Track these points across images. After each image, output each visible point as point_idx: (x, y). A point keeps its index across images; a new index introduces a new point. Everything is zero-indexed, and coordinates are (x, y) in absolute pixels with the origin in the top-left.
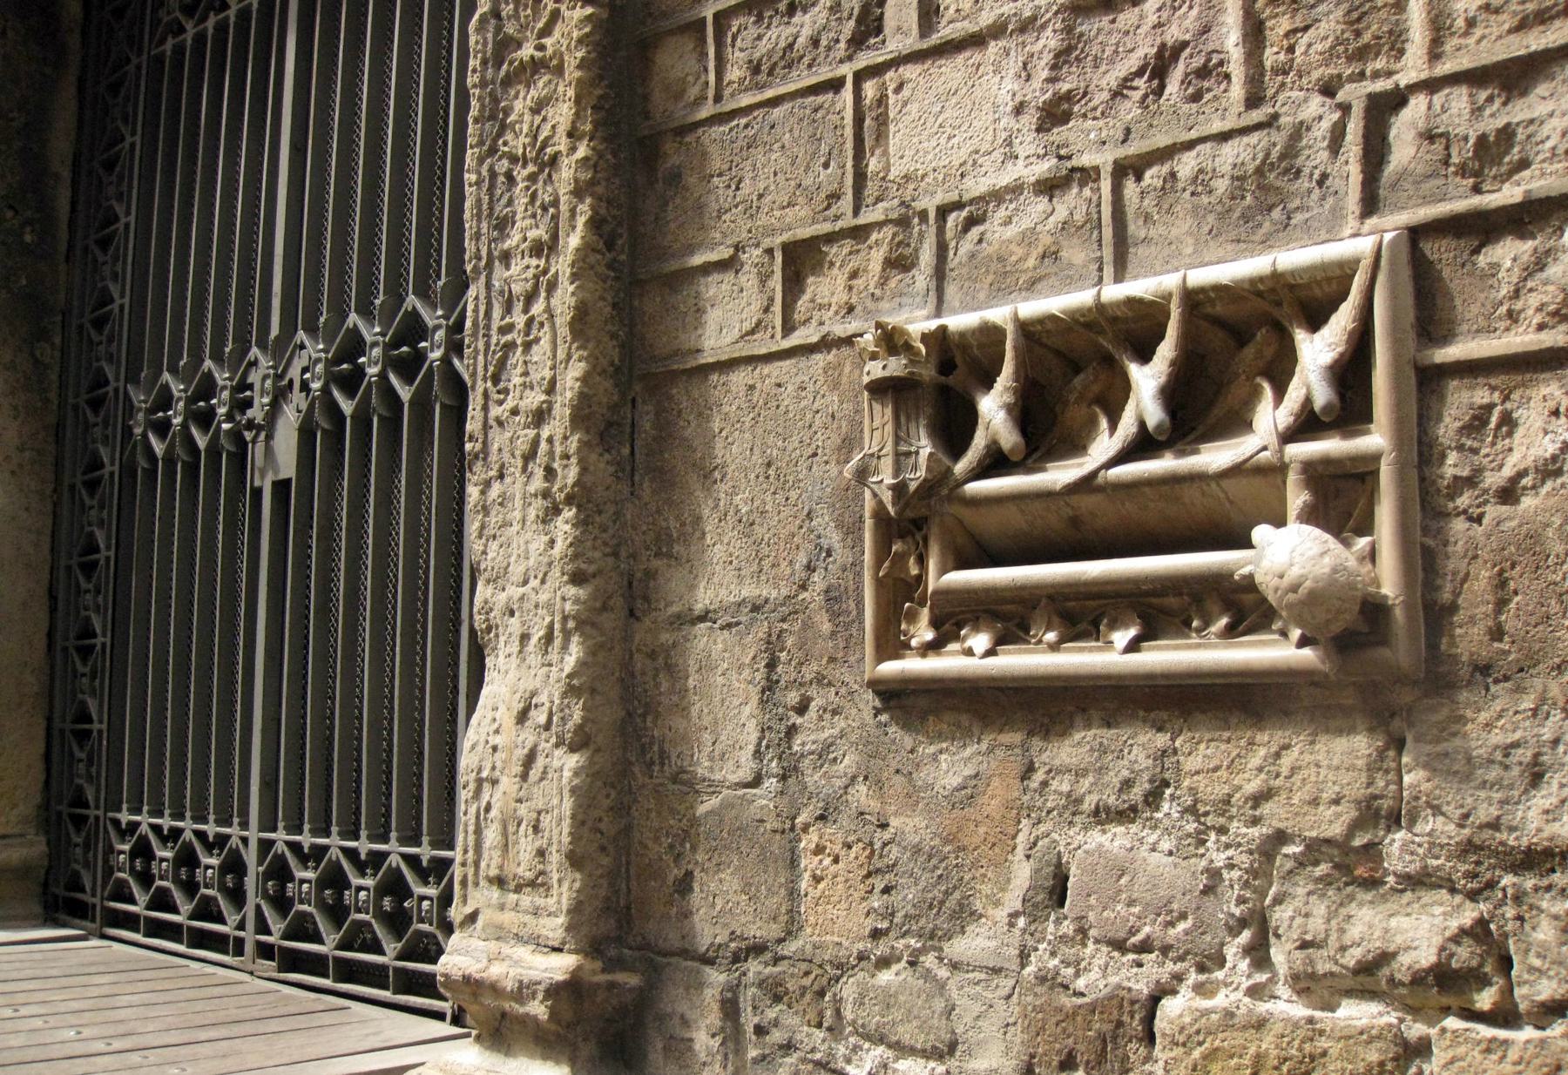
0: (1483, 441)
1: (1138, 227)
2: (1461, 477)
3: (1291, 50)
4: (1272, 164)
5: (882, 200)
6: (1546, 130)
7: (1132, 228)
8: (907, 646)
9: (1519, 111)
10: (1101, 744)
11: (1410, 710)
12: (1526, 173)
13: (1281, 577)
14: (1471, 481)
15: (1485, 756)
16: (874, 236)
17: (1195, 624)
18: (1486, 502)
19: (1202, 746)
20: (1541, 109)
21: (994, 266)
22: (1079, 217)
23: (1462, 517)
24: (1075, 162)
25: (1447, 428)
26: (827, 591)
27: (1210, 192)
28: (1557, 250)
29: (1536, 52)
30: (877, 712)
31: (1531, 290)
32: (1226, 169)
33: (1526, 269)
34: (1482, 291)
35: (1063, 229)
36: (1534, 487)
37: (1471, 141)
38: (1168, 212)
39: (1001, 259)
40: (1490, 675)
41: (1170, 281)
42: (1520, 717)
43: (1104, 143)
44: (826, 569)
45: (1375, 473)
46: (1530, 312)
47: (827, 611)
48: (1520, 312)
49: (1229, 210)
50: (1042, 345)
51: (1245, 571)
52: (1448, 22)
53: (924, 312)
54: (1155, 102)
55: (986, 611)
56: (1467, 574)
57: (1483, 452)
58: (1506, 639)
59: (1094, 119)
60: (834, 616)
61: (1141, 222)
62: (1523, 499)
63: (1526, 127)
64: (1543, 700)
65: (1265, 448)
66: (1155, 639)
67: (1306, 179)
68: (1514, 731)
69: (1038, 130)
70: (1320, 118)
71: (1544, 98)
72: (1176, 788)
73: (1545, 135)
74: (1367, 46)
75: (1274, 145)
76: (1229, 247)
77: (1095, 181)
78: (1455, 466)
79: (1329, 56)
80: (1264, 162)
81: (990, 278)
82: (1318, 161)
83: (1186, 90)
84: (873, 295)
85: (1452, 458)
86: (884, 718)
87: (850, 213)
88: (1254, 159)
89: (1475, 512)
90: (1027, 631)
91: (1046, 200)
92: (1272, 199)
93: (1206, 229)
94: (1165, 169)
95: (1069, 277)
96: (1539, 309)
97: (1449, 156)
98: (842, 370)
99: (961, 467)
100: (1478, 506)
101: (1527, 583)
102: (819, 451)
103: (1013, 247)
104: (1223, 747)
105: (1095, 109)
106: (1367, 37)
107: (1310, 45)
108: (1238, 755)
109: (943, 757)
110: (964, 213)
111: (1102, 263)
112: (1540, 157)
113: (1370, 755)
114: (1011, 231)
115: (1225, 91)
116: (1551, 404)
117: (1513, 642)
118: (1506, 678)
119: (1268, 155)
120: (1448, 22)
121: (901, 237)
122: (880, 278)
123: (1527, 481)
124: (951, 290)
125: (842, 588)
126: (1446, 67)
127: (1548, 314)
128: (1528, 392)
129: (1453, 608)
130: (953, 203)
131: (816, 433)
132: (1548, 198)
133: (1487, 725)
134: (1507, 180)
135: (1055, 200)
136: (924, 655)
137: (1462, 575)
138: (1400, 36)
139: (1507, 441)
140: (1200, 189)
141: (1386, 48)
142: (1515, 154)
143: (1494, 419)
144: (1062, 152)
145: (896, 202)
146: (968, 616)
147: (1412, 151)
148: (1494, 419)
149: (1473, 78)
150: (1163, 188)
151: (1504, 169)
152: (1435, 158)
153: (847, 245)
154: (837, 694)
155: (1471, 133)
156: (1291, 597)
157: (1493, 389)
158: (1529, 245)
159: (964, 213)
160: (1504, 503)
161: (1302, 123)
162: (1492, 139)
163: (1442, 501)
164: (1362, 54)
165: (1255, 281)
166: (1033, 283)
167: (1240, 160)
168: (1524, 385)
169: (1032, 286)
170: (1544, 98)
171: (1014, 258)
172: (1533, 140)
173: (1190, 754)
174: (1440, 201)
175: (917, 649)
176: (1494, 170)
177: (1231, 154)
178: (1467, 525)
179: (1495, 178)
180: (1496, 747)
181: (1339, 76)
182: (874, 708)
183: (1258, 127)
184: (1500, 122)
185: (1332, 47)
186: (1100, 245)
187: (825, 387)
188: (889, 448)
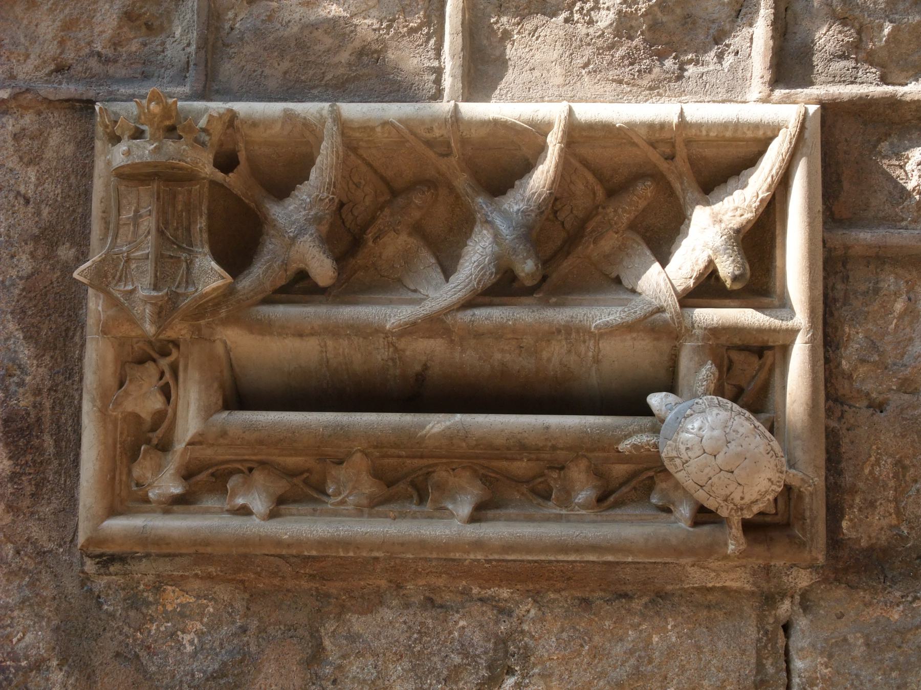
50: (360, 156)
51: (643, 439)
53: (187, 89)
55: (262, 463)
72: (523, 678)
76: (611, 87)
81: (285, 65)
84: (99, 55)
93: (580, 61)
98: (45, 142)
99: (246, 283)
103: (319, 34)
109: (187, 637)
125: (32, 419)
136: (166, 512)
146: (239, 466)
152: (846, 39)
165: (651, 127)
174: (852, 83)
175: (159, 502)
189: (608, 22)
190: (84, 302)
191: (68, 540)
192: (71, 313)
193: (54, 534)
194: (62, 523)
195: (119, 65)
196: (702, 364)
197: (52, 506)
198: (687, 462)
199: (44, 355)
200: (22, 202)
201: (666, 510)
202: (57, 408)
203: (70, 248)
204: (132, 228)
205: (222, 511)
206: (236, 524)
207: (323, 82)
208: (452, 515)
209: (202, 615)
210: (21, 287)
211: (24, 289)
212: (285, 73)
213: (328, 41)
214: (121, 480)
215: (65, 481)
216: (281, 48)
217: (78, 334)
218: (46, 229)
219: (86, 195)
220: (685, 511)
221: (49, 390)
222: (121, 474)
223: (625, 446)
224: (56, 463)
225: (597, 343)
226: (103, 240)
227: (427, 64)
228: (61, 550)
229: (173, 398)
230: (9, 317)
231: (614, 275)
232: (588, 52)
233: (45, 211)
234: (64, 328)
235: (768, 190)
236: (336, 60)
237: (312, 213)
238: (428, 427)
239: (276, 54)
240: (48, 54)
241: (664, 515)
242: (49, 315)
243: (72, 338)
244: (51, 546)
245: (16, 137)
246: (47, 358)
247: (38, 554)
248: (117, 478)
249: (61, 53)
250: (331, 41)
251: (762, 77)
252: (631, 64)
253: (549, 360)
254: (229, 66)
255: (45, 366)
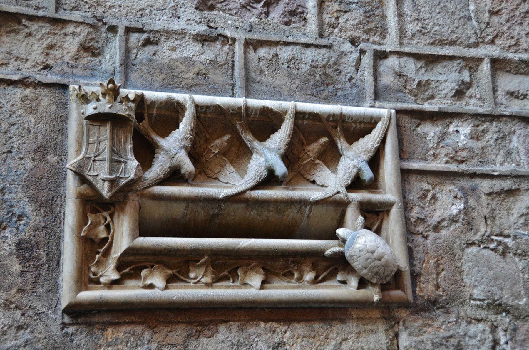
0: (425, 204)
1: (256, 75)
2: (421, 219)
3: (337, 18)
4: (330, 65)
5: (77, 10)
6: (442, 86)
7: (252, 74)
8: (98, 282)
9: (431, 76)
10: (238, 341)
11: (404, 322)
12: (434, 101)
13: (373, 253)
14: (423, 220)
15: (439, 342)
16: (71, 28)
17: (296, 275)
18: (429, 231)
19: (299, 341)
20: (441, 78)
21: (165, 70)
22: (221, 60)
23: (420, 236)
24: (220, 31)
25: (413, 196)
26: (18, 244)
27: (298, 69)
28: (448, 134)
29: (441, 55)
30: (64, 325)
31: (442, 147)
32: (309, 60)
33: (439, 138)
34: (421, 143)
35: (210, 63)
36: (447, 227)
37: (416, 82)
38: (273, 72)
39: (170, 68)
40: (435, 306)
41: (288, 105)
42: (450, 325)
43: (237, 28)
44: (18, 228)
45: (388, 212)
46: (443, 156)
47: (18, 257)
48: (438, 154)
49: (308, 80)
51: (337, 249)
52: (404, 32)
54: (266, 18)
56: (424, 261)
57: (426, 209)
58: (441, 290)
59: (230, 14)
60: (23, 261)
61: (258, 73)
62: (441, 231)
63: (435, 83)
64: (458, 318)
65: (338, 193)
66: (270, 283)
67: (344, 77)
68: (449, 331)
69: (196, 8)
70: (352, 53)
71: (441, 74)
73: (442, 88)
74: (371, 29)
75: (332, 57)
76: (308, 97)
77: (231, 45)
78: (418, 213)
79: (356, 27)
80: (327, 64)
81: (163, 76)
82: (349, 71)
83: (283, 18)
84: (68, 63)
85: (416, 210)
86: (70, 330)
87: (52, 9)
88: (322, 60)
89: (425, 234)
90: (188, 277)
91: (200, 45)
92: (328, 81)
93: (295, 86)
94: (273, 51)
95: (214, 89)
96: (447, 155)
97: (406, 85)
98: (39, 103)
100: (426, 232)
101: (447, 266)
102: (14, 150)
104: (311, 340)
105: (231, 9)
106: (371, 26)
107: (347, 20)
108: (320, 345)
110: (145, 36)
111: (233, 86)
112: (439, 96)
113: (388, 343)
114: (175, 55)
115: (303, 26)
116: (453, 194)
117: (444, 291)
118: (442, 307)
119: (329, 60)
120: (404, 32)
121: (93, 36)
122: (75, 55)
123: (445, 223)
124: (134, 76)
125: (33, 242)
126: (406, 49)
127: (450, 158)
128: (442, 187)
129: (419, 275)
130: (137, 29)
131: (11, 138)
132: (447, 112)
133: (438, 328)
134: (426, 101)
135: (205, 47)
137: (423, 260)
138: (384, 30)
139: (433, 206)
140: (292, 66)
141: (379, 33)
142: (429, 92)
143: (430, 196)
144: (212, 25)
145: (89, 14)
147: (392, 79)
148: (430, 196)
149: (417, 57)
150: (271, 60)
151: (425, 97)
153: (47, 28)
154: (23, 315)
155: (416, 79)
156: (377, 263)
157: (429, 184)
158: (437, 129)
159: (145, 36)
160: (435, 232)
161: (343, 52)
162: (423, 83)
163: (413, 228)
164: (368, 31)
166: (192, 86)
167: (316, 59)
168: (440, 184)
169: (190, 88)
170: (441, 74)
171: (178, 70)
172: (438, 89)
173: (293, 345)
174: (405, 102)
175: (105, 284)
176: (422, 95)
177: (310, 54)
178: (423, 239)
179: (422, 99)
180: (443, 338)
181: (359, 38)
182: (63, 323)
183: (325, 47)
184: (425, 78)
185: (357, 24)
186: (232, 78)
187: (22, 111)
188: (106, 155)
189: (306, 70)
190: (62, 184)
191: (54, 306)
192: (55, 189)
193: (45, 304)
194: (50, 297)
195: (79, 69)
196: (358, 217)
197: (44, 288)
198: (359, 257)
199: (40, 210)
200: (27, 132)
201: (344, 282)
202: (48, 237)
203: (55, 156)
204: (96, 144)
205: (139, 287)
206: (148, 293)
207: (181, 86)
208: (251, 286)
209: (128, 342)
210: (26, 175)
211: (28, 176)
212: (163, 80)
213: (183, 67)
214: (85, 273)
215: (52, 275)
216: (161, 68)
217: (59, 199)
218: (41, 146)
219: (63, 130)
220: (354, 282)
221: (44, 227)
222: (85, 270)
223: (328, 252)
224: (46, 266)
225: (311, 207)
226: (78, 152)
227: (228, 81)
228: (50, 312)
229: (112, 231)
230: (19, 190)
231: (312, 179)
232: (298, 81)
233: (40, 137)
234: (51, 196)
235: (378, 143)
236: (187, 76)
237: (182, 144)
238: (241, 244)
239: (158, 71)
240: (39, 61)
241: (343, 285)
242: (43, 189)
243: (56, 201)
244: (44, 310)
245: (22, 100)
246: (42, 211)
247: (36, 314)
248: (83, 272)
249: (47, 61)
250: (184, 67)
251: (371, 97)
252: (316, 88)
253: (288, 215)
254: (136, 74)
255: (41, 216)
